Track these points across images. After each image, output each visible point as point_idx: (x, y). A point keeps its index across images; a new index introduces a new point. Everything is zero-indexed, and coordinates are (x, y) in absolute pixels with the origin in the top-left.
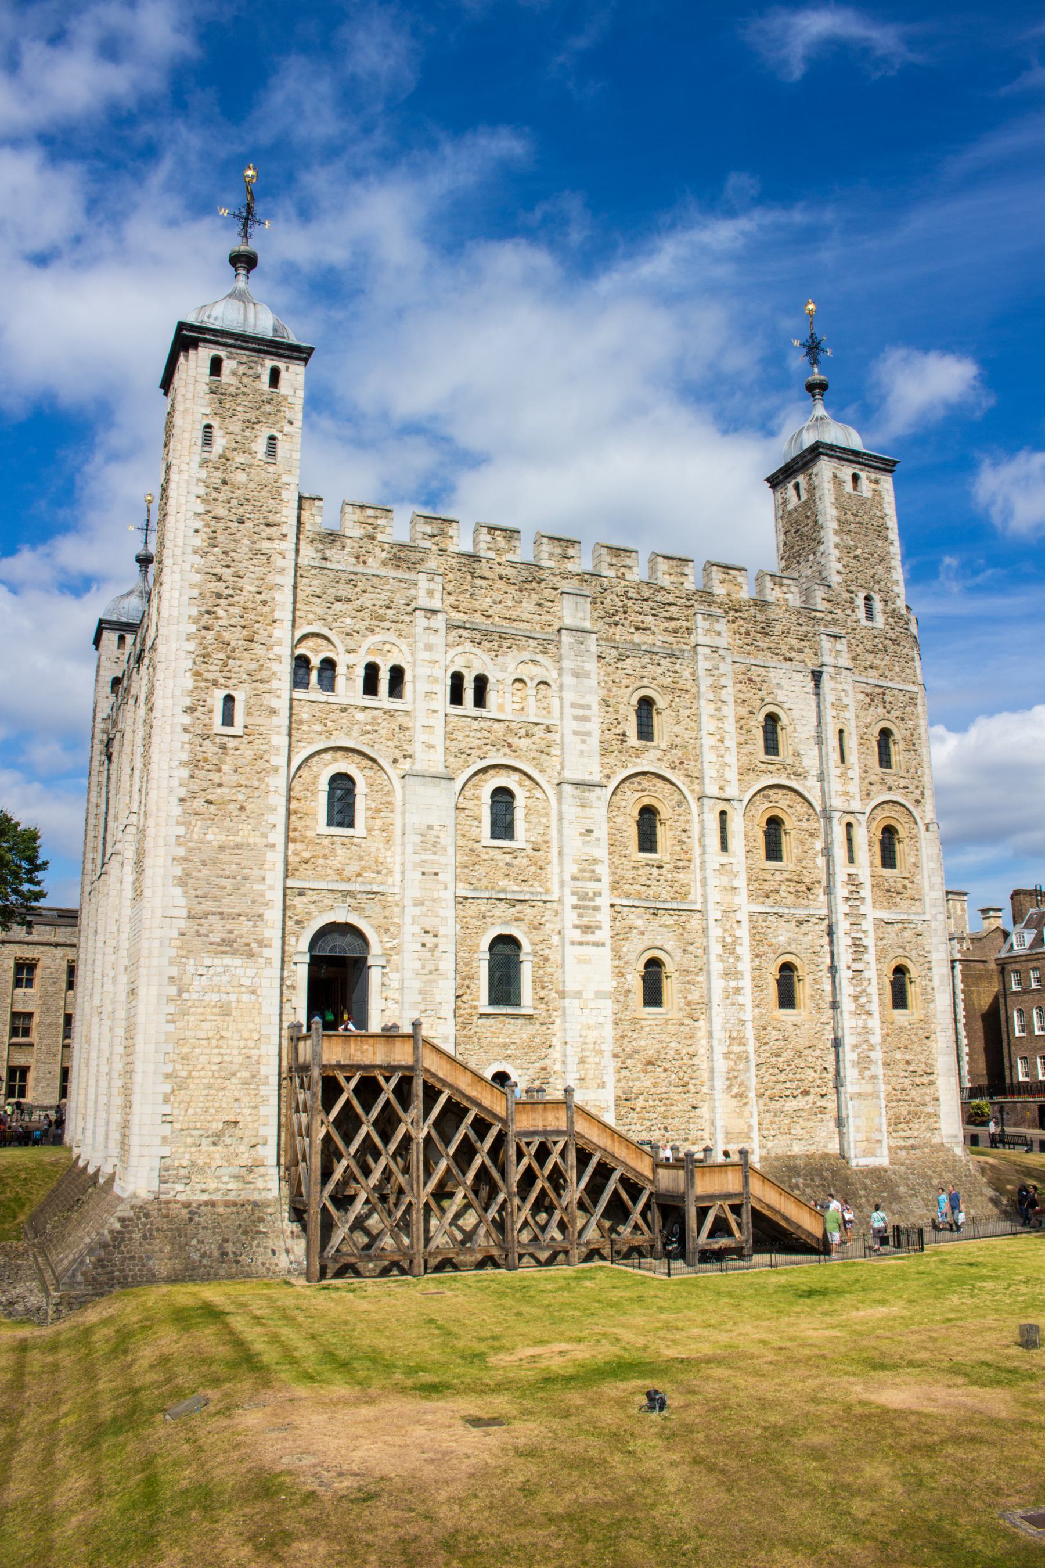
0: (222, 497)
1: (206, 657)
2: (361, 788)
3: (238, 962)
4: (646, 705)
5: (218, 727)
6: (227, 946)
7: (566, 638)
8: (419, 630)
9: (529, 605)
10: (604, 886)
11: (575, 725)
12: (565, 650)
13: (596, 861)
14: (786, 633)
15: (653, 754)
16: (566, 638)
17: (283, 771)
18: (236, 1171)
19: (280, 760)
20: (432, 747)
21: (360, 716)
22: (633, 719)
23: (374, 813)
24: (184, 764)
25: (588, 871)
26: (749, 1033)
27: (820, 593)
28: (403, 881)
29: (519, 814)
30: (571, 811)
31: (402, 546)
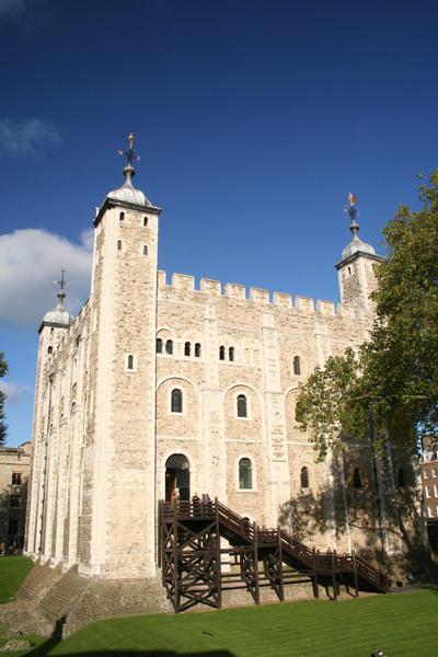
2: (184, 396)
3: (136, 471)
4: (296, 358)
5: (126, 369)
6: (132, 464)
7: (265, 332)
12: (265, 337)
13: (281, 426)
14: (350, 329)
16: (265, 332)
17: (154, 389)
18: (137, 565)
19: (152, 384)
21: (184, 365)
22: (292, 366)
23: (191, 406)
24: (113, 385)
25: (278, 431)
26: (345, 498)
27: (362, 313)
28: (203, 435)
30: (270, 404)
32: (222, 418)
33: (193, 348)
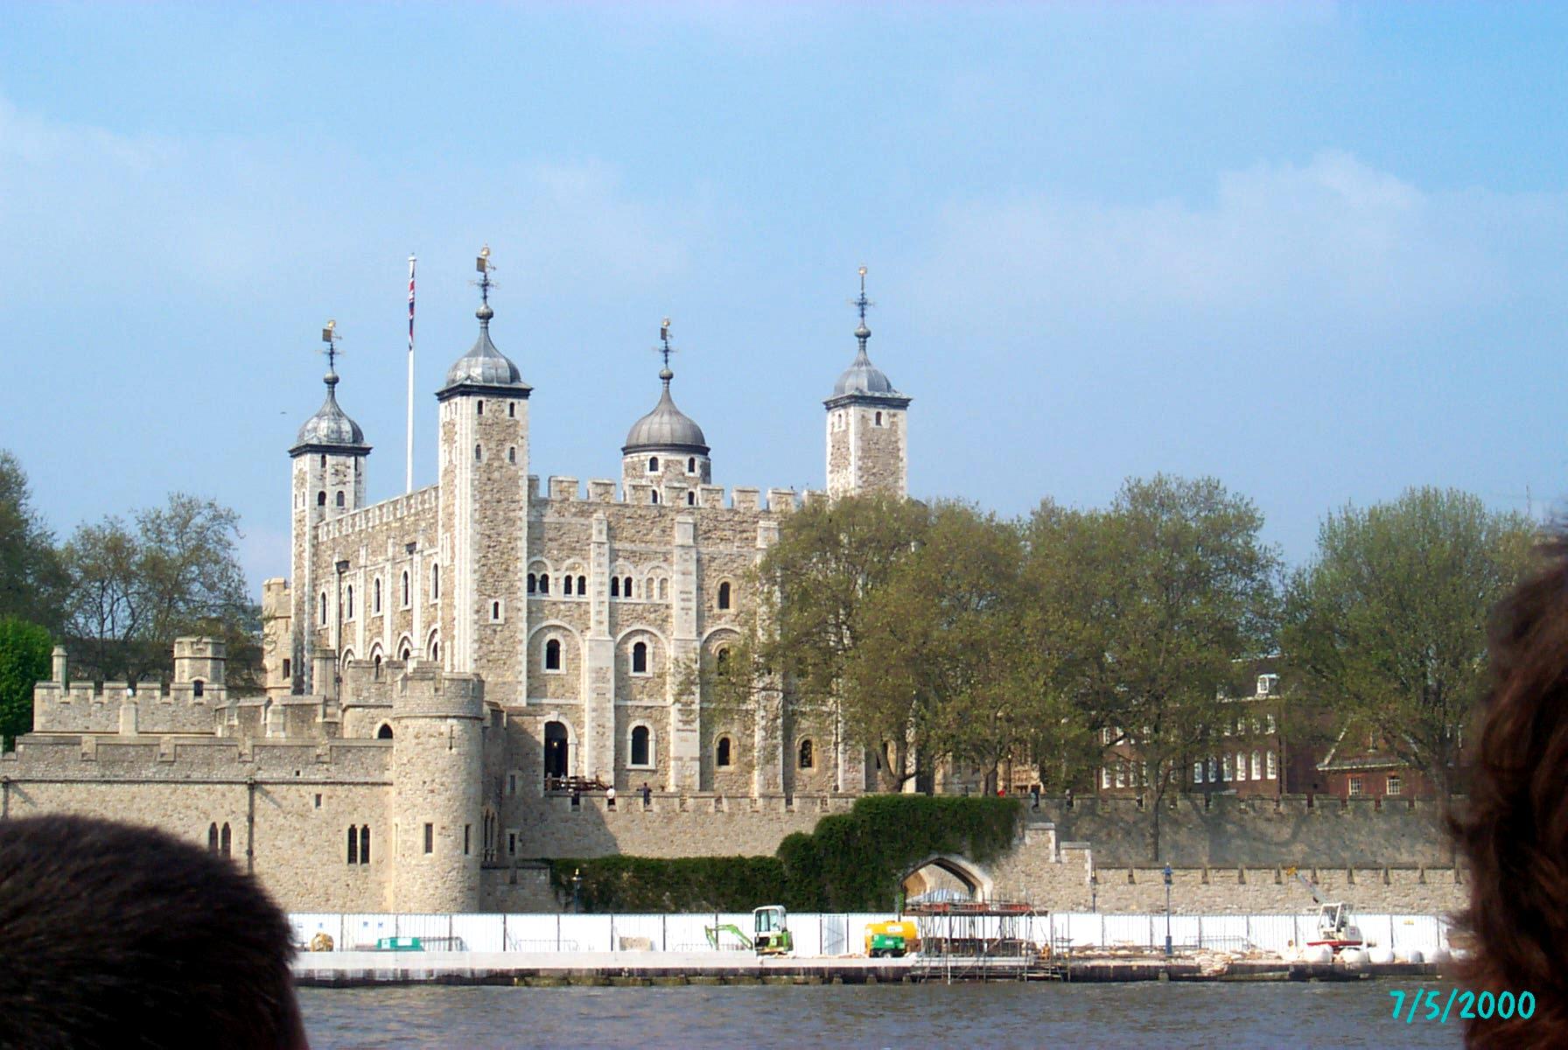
0: (488, 488)
1: (483, 581)
2: (562, 648)
4: (725, 589)
5: (491, 620)
7: (677, 552)
8: (592, 554)
9: (656, 531)
10: (697, 698)
11: (682, 604)
15: (727, 618)
16: (677, 552)
20: (601, 623)
23: (570, 661)
29: (649, 658)
31: (584, 503)
32: (611, 675)
33: (575, 583)
